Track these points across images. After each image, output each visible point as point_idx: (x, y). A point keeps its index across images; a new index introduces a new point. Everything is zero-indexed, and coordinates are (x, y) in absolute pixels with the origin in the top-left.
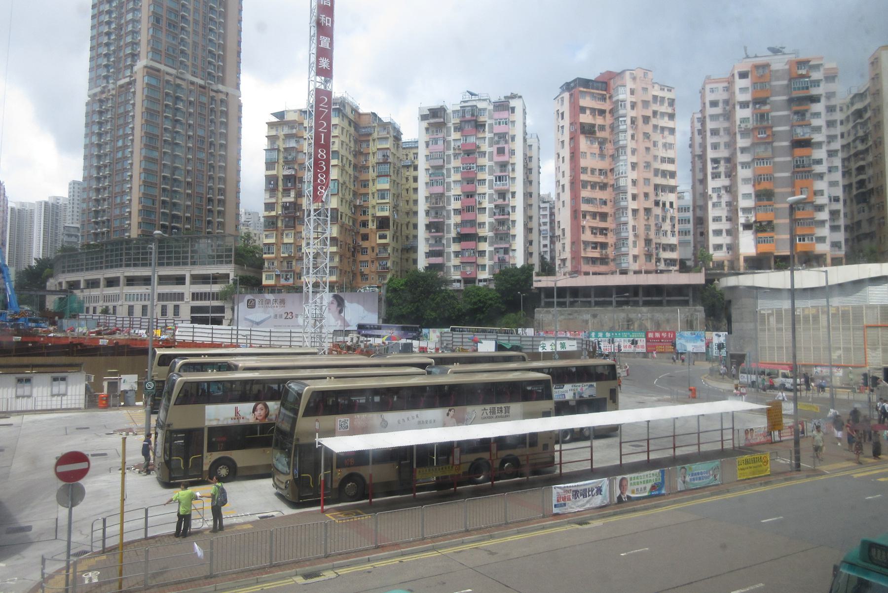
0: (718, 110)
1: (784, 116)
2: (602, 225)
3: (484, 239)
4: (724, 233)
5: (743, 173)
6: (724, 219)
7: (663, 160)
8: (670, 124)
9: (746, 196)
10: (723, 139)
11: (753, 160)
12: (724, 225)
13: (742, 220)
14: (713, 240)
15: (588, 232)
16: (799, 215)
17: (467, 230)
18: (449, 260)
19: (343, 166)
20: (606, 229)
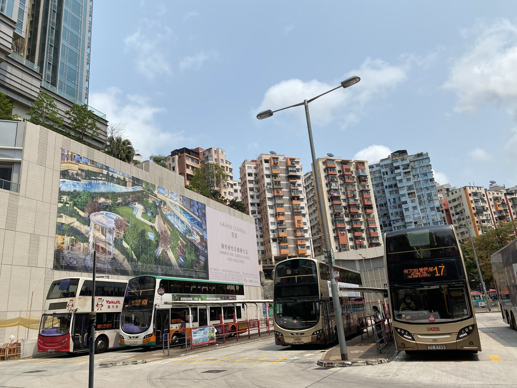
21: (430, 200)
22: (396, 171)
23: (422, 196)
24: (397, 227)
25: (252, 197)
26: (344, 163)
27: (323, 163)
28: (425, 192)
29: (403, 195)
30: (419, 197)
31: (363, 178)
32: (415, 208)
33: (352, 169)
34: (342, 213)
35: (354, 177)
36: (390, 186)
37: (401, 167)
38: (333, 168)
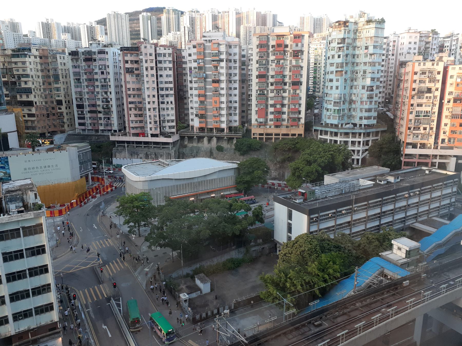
2: (140, 113)
3: (100, 112)
15: (133, 116)
17: (94, 109)
18: (87, 121)
19: (33, 80)
20: (142, 114)
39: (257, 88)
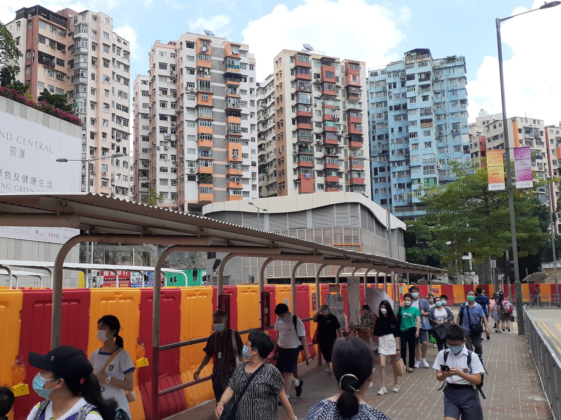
0: (167, 72)
1: (221, 87)
4: (170, 182)
5: (189, 130)
6: (169, 170)
7: (118, 107)
8: (125, 75)
9: (191, 150)
10: (170, 99)
11: (197, 120)
12: (170, 176)
13: (187, 171)
14: (160, 188)
16: (232, 171)
21: (456, 133)
22: (409, 83)
23: (444, 127)
24: (399, 172)
25: (163, 105)
26: (327, 61)
27: (292, 58)
28: (450, 120)
29: (413, 123)
30: (439, 127)
31: (354, 89)
32: (428, 144)
33: (338, 72)
34: (312, 145)
35: (338, 87)
36: (397, 108)
37: (417, 77)
38: (306, 69)
39: (295, 141)
